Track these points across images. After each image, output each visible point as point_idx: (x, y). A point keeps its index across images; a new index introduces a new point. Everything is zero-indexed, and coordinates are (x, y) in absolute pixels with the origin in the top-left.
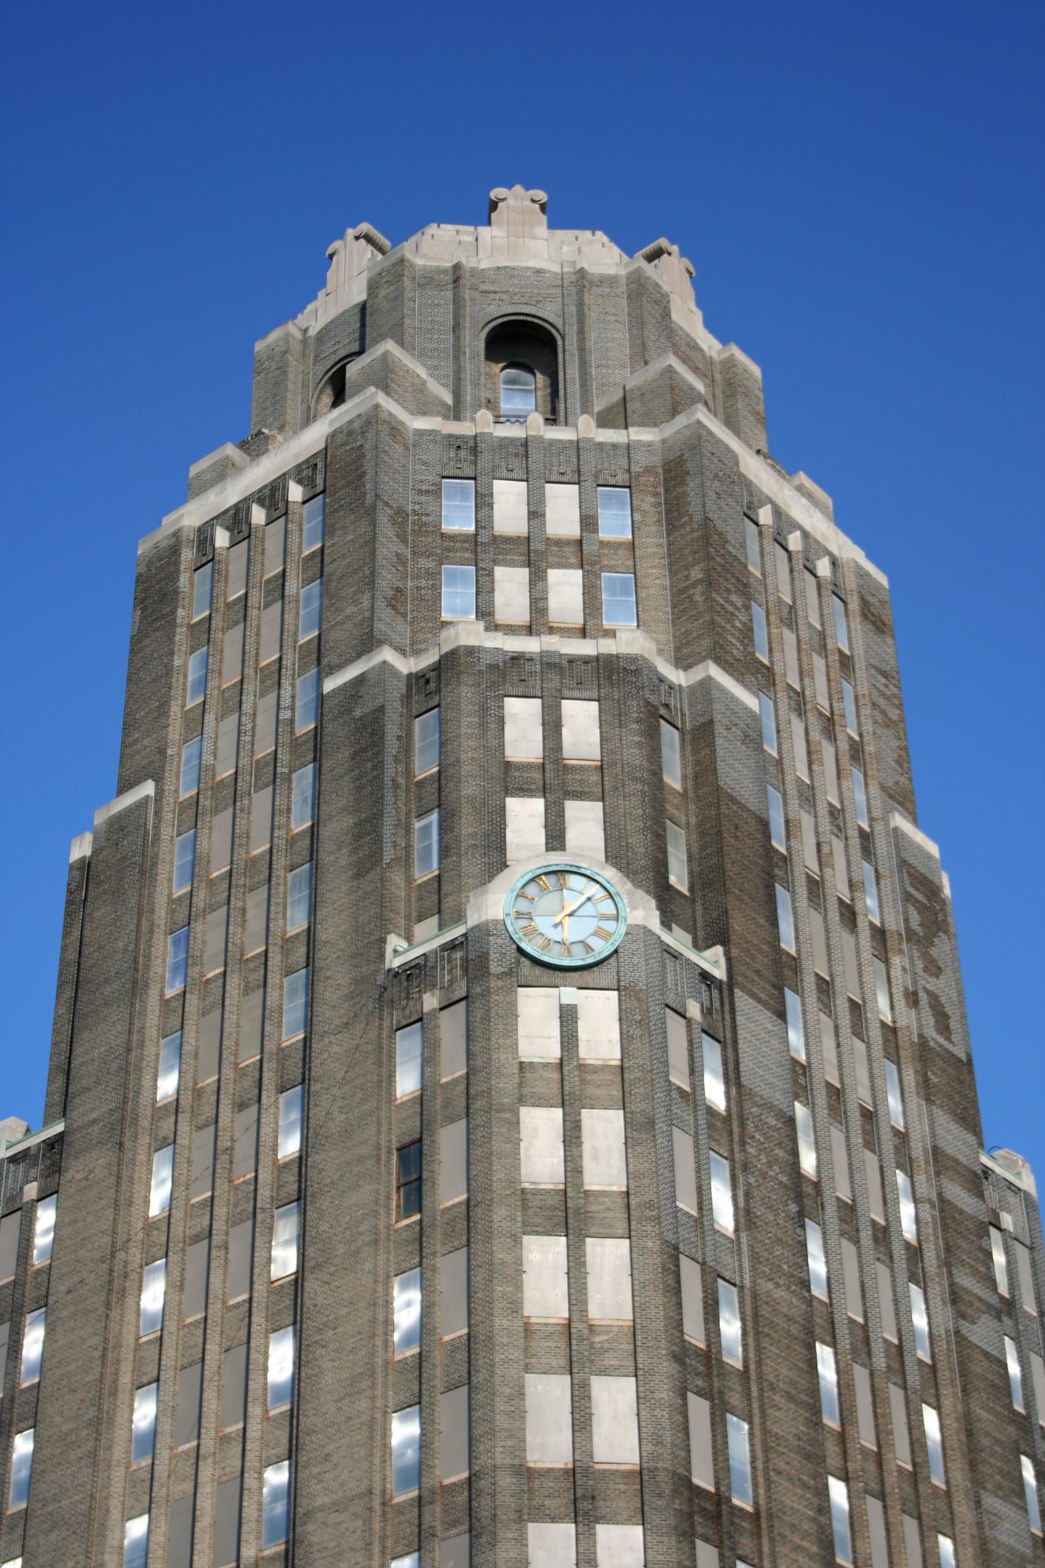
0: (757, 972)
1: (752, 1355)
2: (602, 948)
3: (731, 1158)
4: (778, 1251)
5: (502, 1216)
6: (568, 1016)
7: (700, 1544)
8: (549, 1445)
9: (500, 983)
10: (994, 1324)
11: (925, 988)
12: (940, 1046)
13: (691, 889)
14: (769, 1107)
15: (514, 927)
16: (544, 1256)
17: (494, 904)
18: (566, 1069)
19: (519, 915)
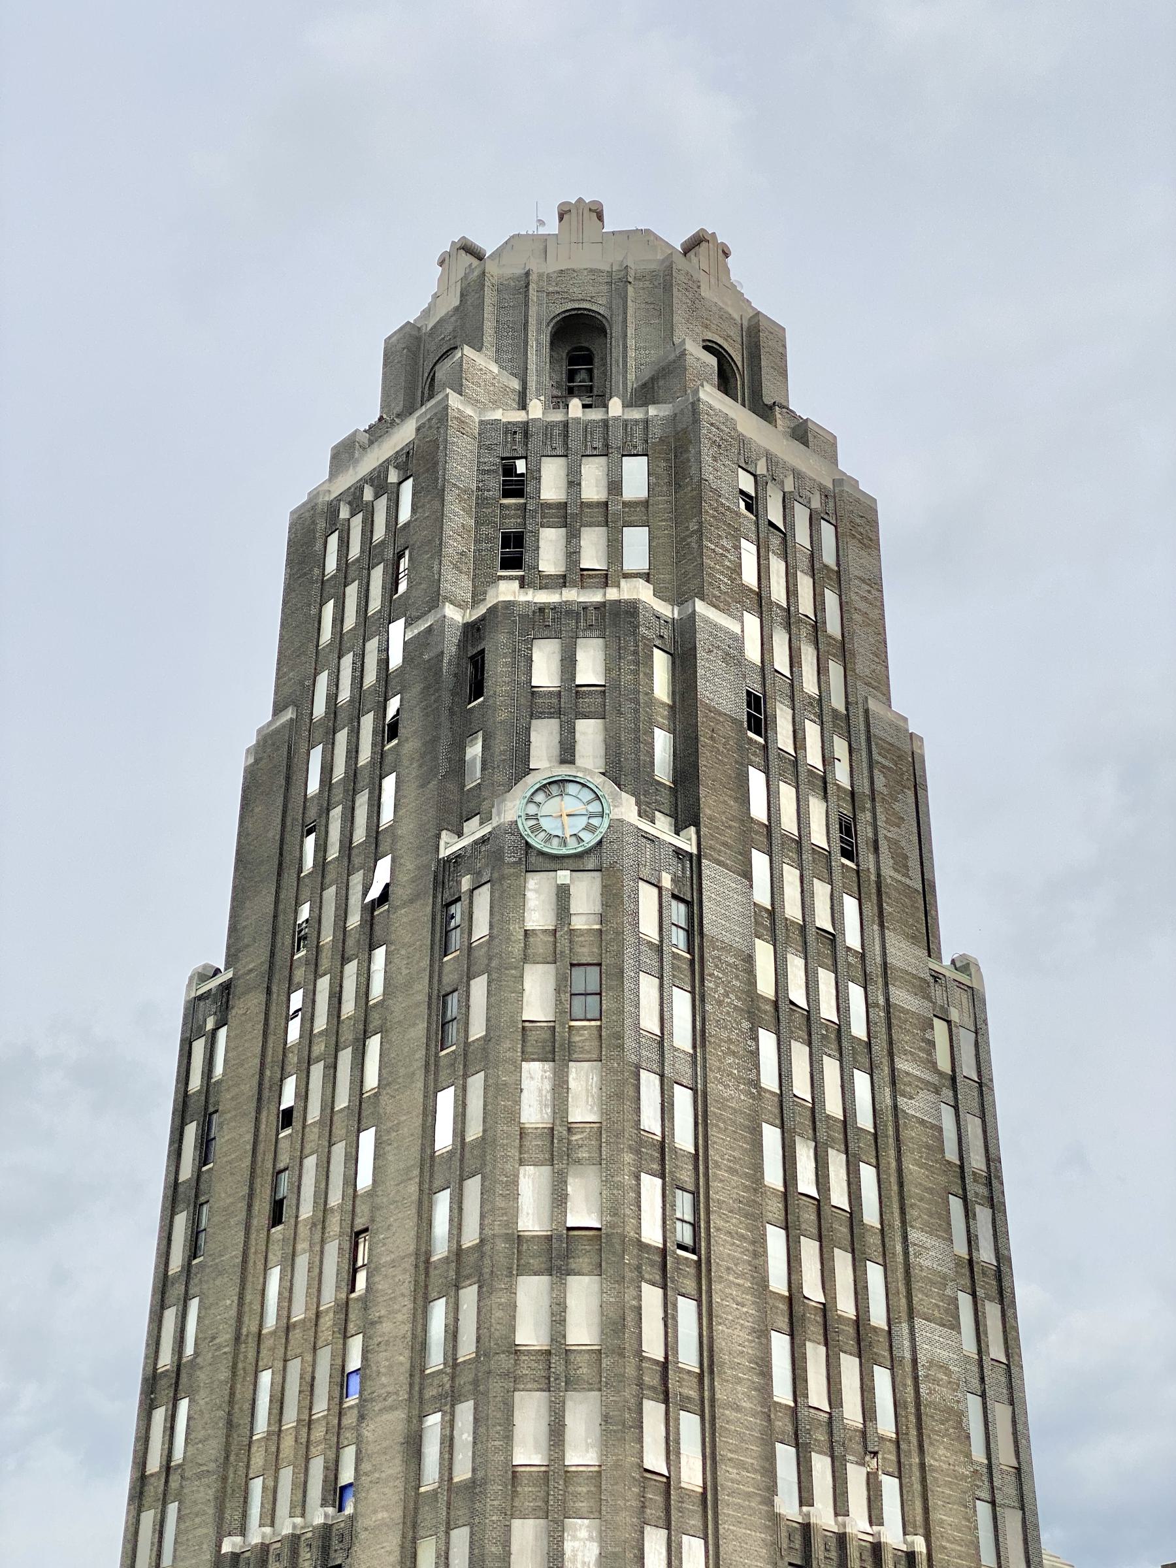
0: (725, 844)
1: (700, 1142)
2: (590, 839)
3: (693, 993)
4: (730, 1060)
5: (508, 1047)
6: (563, 894)
7: (645, 1286)
8: (532, 1218)
9: (512, 870)
10: (932, 1097)
11: (886, 837)
12: (898, 881)
13: (673, 782)
14: (727, 948)
15: (524, 826)
16: (535, 1077)
17: (511, 809)
18: (558, 934)
19: (528, 817)
